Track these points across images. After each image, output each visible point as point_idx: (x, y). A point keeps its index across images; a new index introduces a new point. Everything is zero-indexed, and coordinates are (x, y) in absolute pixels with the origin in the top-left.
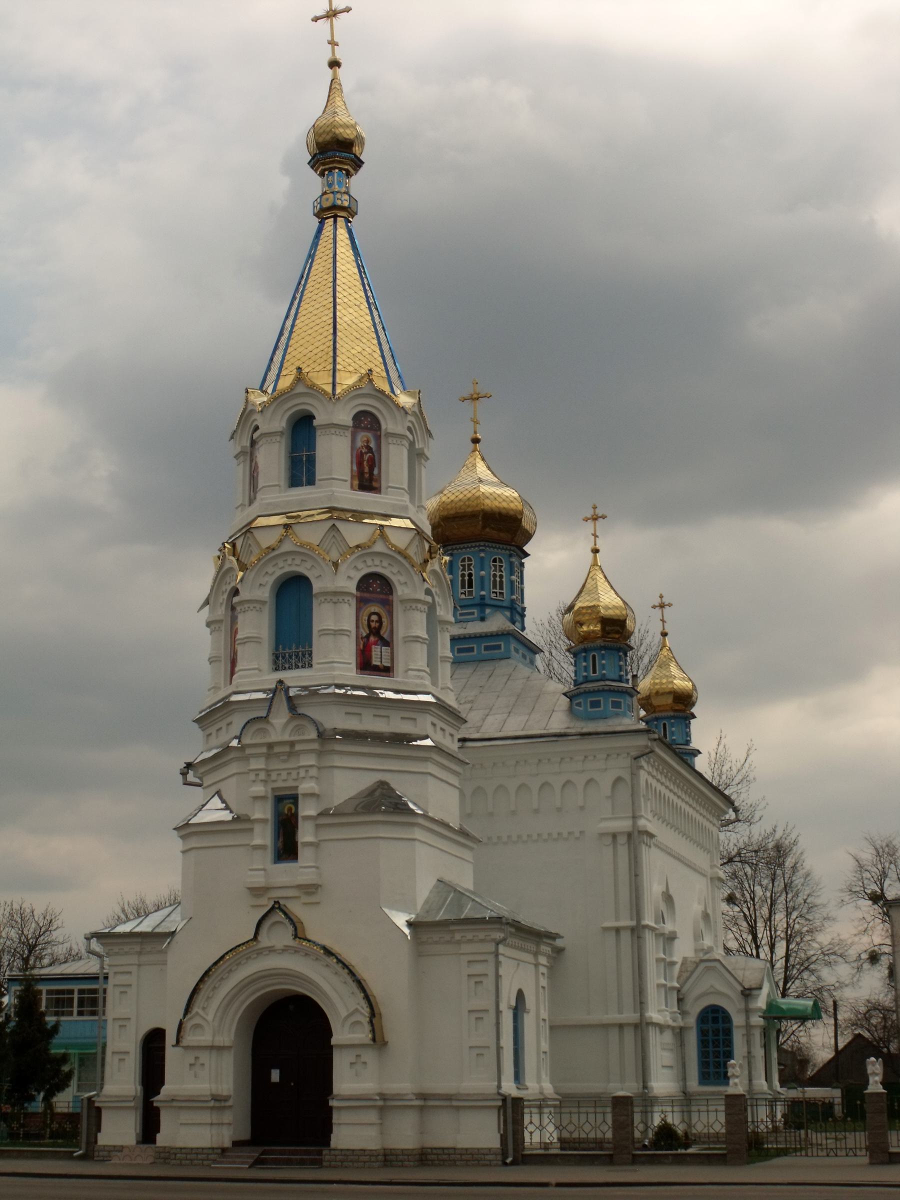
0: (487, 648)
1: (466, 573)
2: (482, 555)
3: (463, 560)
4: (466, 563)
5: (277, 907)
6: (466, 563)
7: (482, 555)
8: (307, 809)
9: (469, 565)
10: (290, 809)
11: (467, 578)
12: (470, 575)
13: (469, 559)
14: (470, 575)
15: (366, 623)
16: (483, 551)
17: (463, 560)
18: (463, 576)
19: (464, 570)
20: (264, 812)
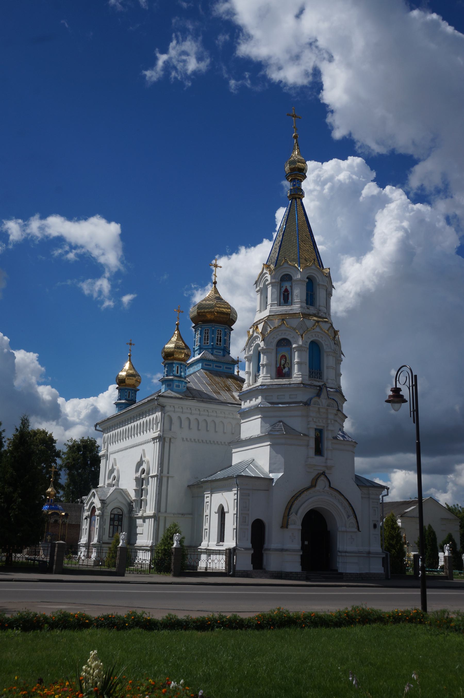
0: (216, 366)
1: (219, 336)
2: (213, 328)
3: (206, 330)
4: (207, 331)
5: (324, 473)
6: (207, 331)
7: (213, 328)
8: (327, 435)
9: (208, 332)
10: (318, 434)
11: (219, 338)
12: (208, 336)
13: (208, 330)
14: (208, 336)
15: (287, 359)
16: (214, 327)
17: (206, 330)
18: (205, 336)
19: (218, 334)
20: (312, 434)
